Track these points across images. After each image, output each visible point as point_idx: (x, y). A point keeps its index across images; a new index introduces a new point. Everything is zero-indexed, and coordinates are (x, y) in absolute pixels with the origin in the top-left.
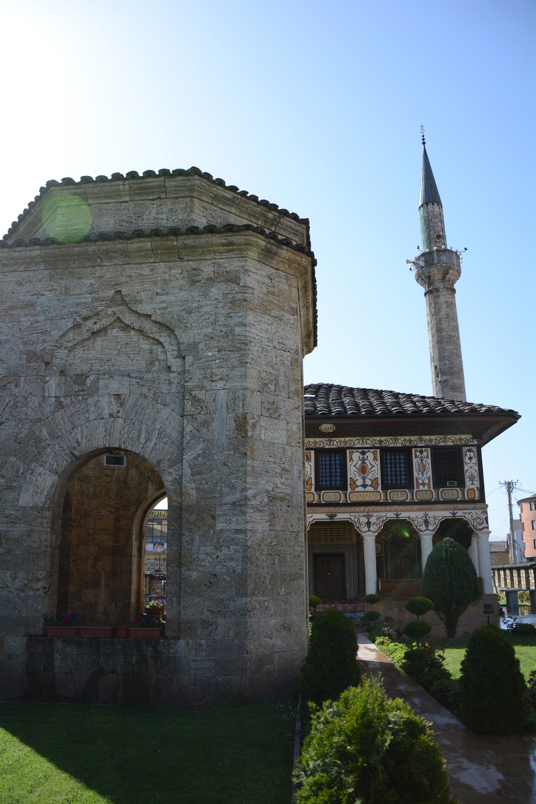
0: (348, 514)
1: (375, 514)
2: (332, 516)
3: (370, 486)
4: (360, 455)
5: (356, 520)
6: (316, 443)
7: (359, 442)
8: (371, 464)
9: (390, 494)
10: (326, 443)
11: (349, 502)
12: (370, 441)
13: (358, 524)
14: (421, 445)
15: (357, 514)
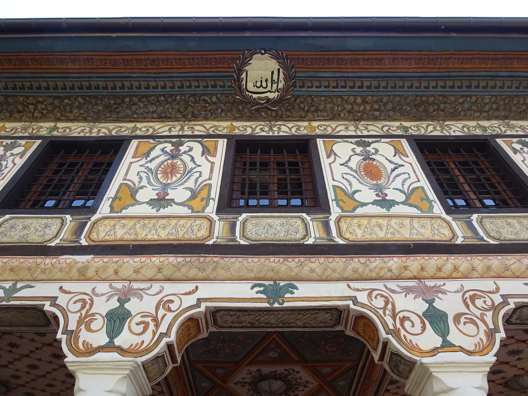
0: (343, 285)
1: (451, 285)
2: (275, 292)
3: (403, 203)
4: (355, 146)
5: (379, 303)
6: (233, 128)
7: (347, 128)
8: (391, 162)
9: (481, 223)
10: (262, 129)
11: (341, 242)
12: (375, 128)
13: (389, 320)
14: (514, 133)
15: (379, 285)
